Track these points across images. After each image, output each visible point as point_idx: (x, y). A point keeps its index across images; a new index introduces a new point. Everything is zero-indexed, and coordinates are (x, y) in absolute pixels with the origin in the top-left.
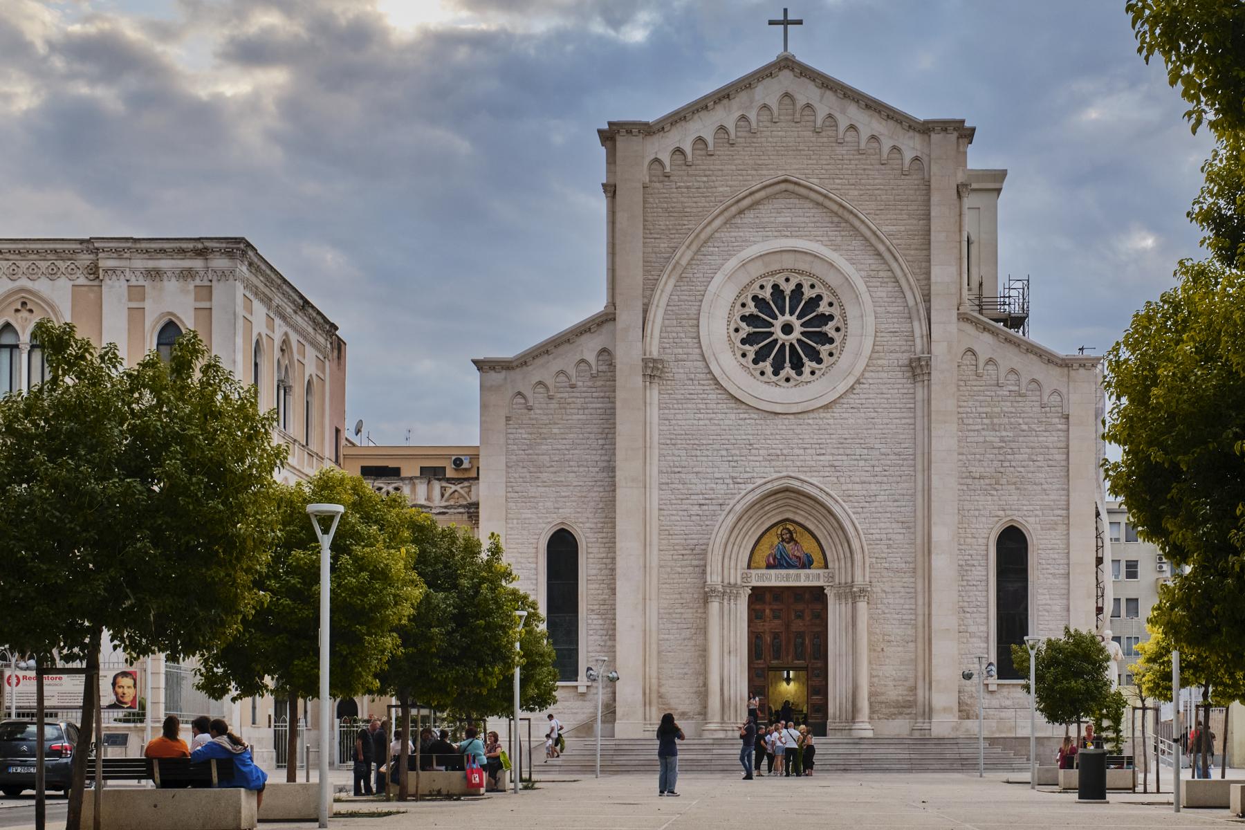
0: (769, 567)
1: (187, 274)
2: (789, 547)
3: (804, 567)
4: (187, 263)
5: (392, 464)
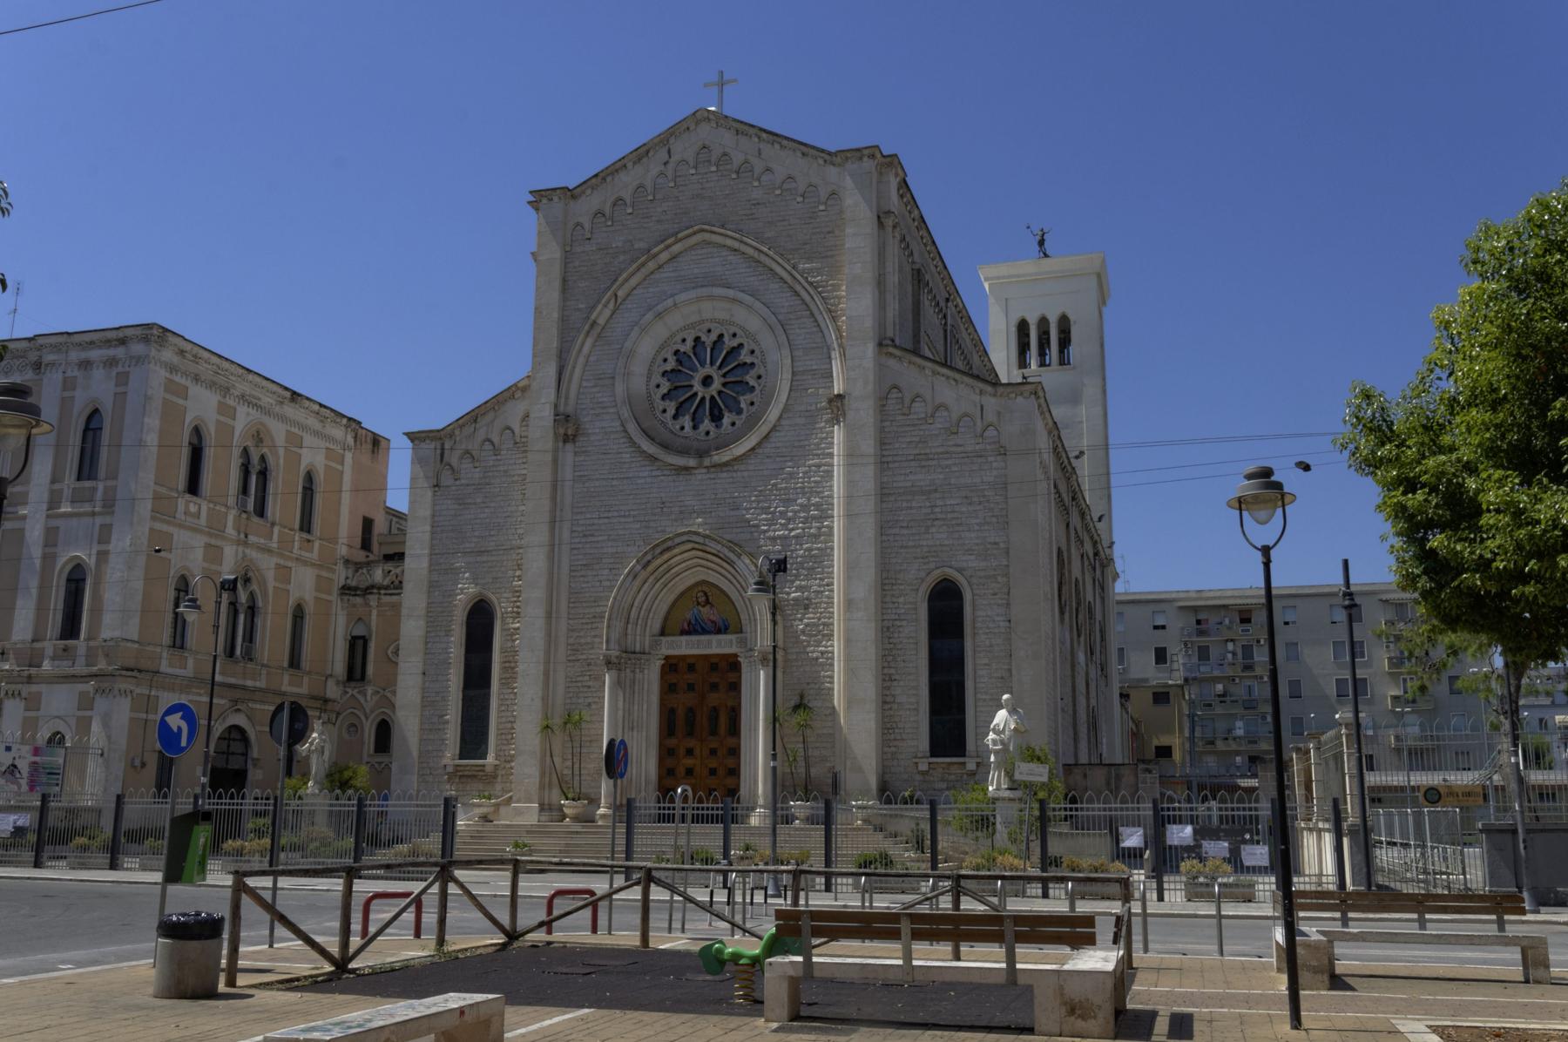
0: (683, 633)
2: (705, 610)
3: (719, 632)
4: (111, 352)
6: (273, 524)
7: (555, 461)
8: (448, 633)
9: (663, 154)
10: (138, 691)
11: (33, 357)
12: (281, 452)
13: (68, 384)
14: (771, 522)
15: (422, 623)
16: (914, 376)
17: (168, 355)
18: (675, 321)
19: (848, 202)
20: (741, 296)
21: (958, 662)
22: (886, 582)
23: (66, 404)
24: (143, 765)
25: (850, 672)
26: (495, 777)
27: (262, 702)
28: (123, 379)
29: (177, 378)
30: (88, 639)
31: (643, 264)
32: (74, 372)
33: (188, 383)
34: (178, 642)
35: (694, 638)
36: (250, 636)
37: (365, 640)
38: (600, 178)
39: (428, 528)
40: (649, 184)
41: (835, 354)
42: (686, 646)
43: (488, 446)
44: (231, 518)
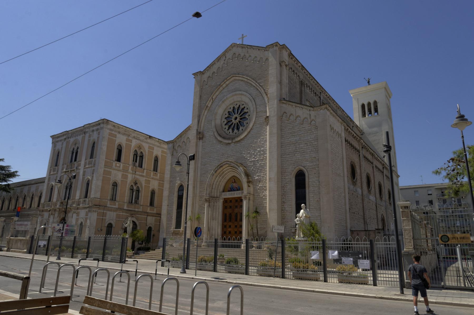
0: (229, 191)
2: (234, 184)
3: (238, 190)
6: (144, 169)
7: (197, 145)
9: (224, 58)
10: (100, 211)
11: (84, 131)
12: (147, 151)
13: (90, 136)
14: (251, 157)
16: (290, 108)
17: (109, 127)
18: (228, 103)
19: (270, 60)
20: (243, 93)
22: (281, 172)
23: (89, 140)
24: (101, 230)
25: (270, 200)
27: (141, 215)
28: (99, 134)
29: (113, 132)
31: (219, 88)
32: (91, 133)
33: (117, 134)
34: (114, 199)
36: (137, 197)
38: (209, 67)
41: (267, 105)
42: (229, 195)
43: (184, 143)
44: (130, 168)
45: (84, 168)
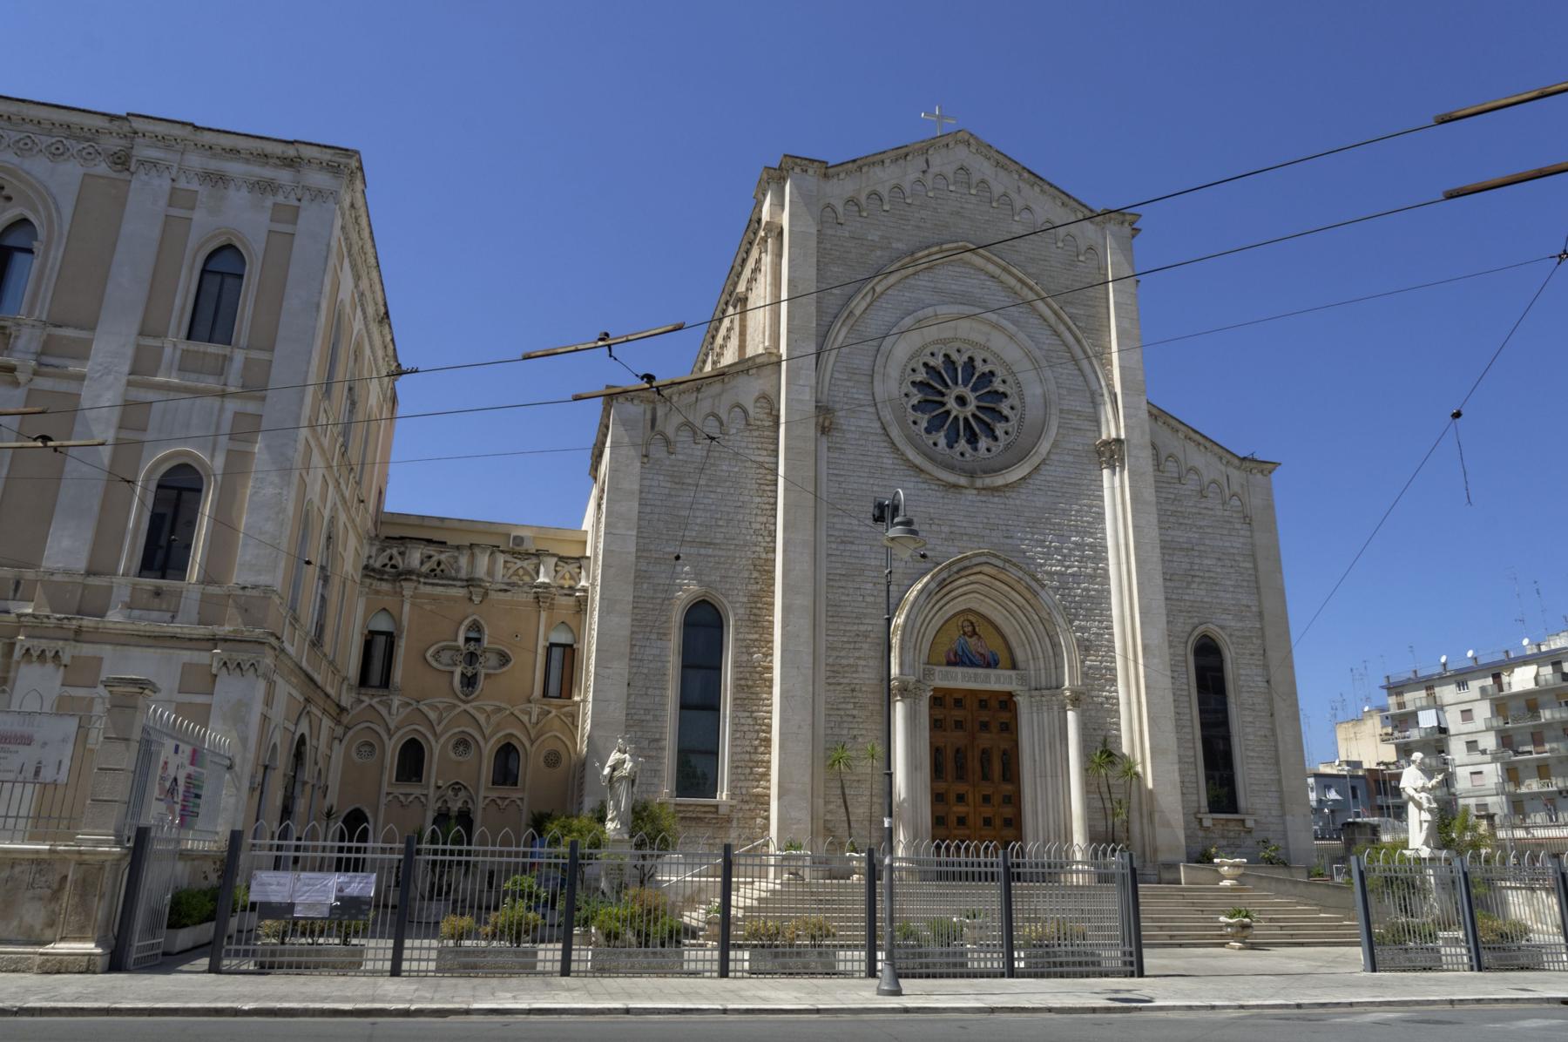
0: (949, 663)
1: (265, 187)
3: (988, 666)
4: (268, 173)
5: (436, 536)
8: (663, 636)
11: (113, 144)
14: (1048, 556)
15: (628, 621)
21: (1225, 723)
26: (729, 820)
30: (207, 579)
35: (959, 670)
37: (391, 638)
38: (858, 165)
39: (636, 505)
40: (907, 187)
42: (962, 679)
45: (129, 383)
